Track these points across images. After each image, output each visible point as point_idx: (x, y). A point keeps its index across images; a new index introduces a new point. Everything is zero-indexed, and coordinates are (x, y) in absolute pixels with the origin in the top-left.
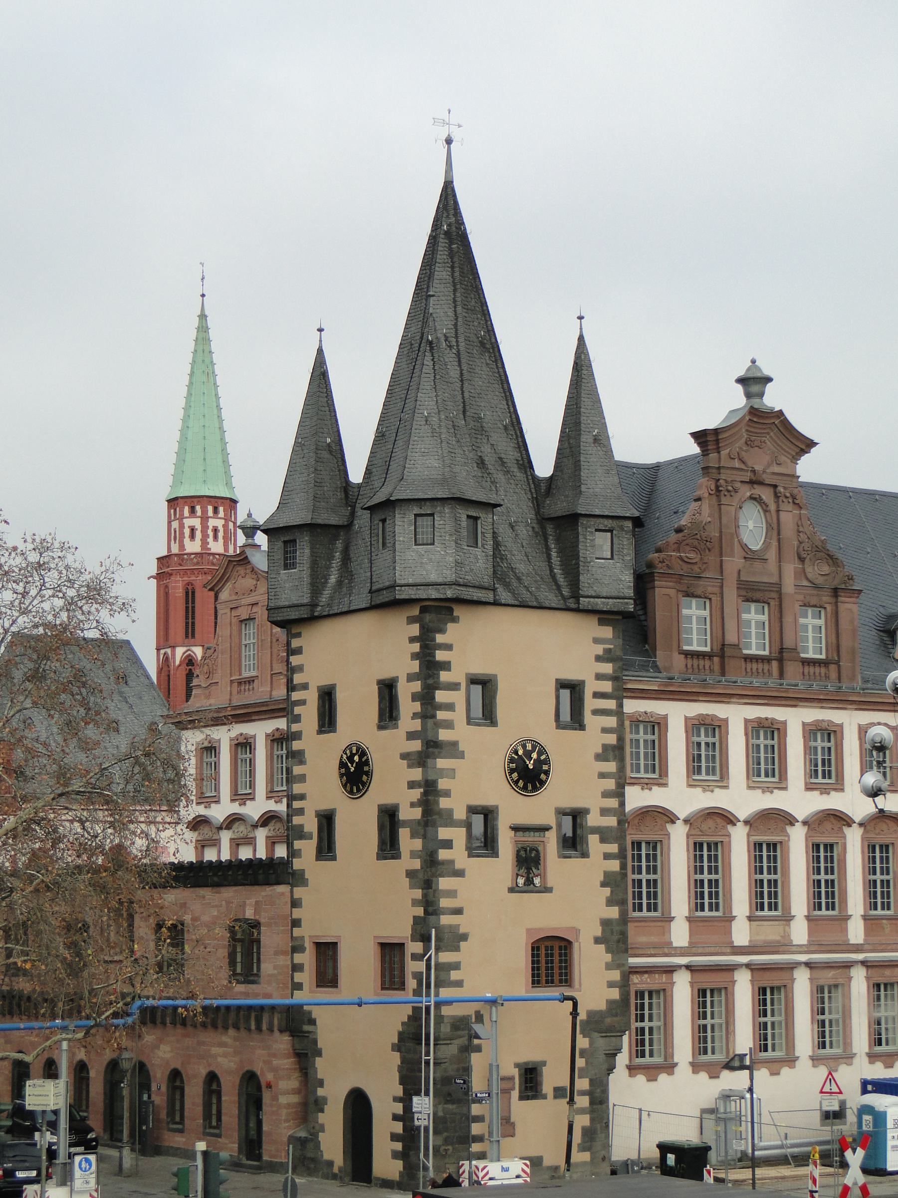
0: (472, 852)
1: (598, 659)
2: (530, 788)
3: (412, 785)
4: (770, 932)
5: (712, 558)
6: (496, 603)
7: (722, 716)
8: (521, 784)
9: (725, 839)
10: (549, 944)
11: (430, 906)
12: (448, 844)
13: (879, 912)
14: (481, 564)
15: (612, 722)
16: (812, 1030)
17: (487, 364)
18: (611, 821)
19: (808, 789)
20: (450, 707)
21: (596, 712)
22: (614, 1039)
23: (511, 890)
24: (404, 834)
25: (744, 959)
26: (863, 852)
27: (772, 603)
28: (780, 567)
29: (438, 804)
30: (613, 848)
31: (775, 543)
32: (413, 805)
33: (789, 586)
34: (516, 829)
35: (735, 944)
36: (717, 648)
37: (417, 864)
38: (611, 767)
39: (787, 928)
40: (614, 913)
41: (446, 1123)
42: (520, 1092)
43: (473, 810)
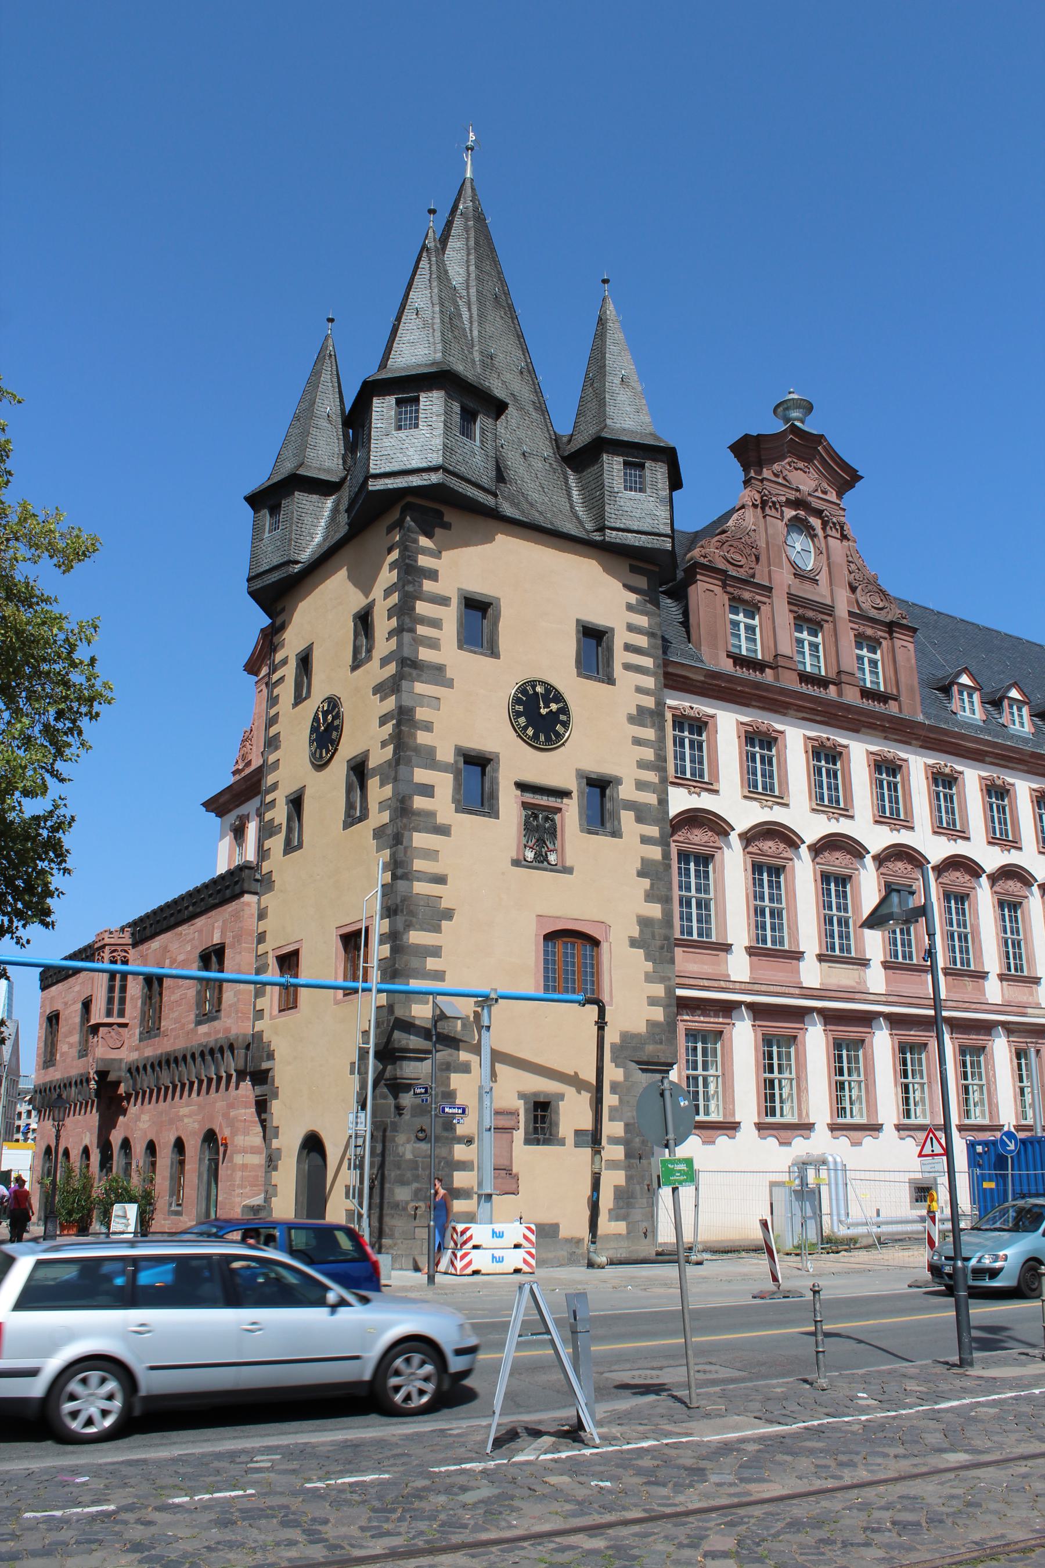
0: (463, 806)
2: (542, 738)
4: (842, 976)
8: (530, 732)
11: (399, 869)
12: (428, 791)
15: (649, 682)
16: (896, 1094)
20: (436, 623)
21: (628, 667)
23: (516, 863)
28: (832, 590)
29: (415, 738)
30: (654, 831)
31: (825, 569)
32: (384, 744)
39: (862, 973)
40: (655, 911)
41: (416, 1169)
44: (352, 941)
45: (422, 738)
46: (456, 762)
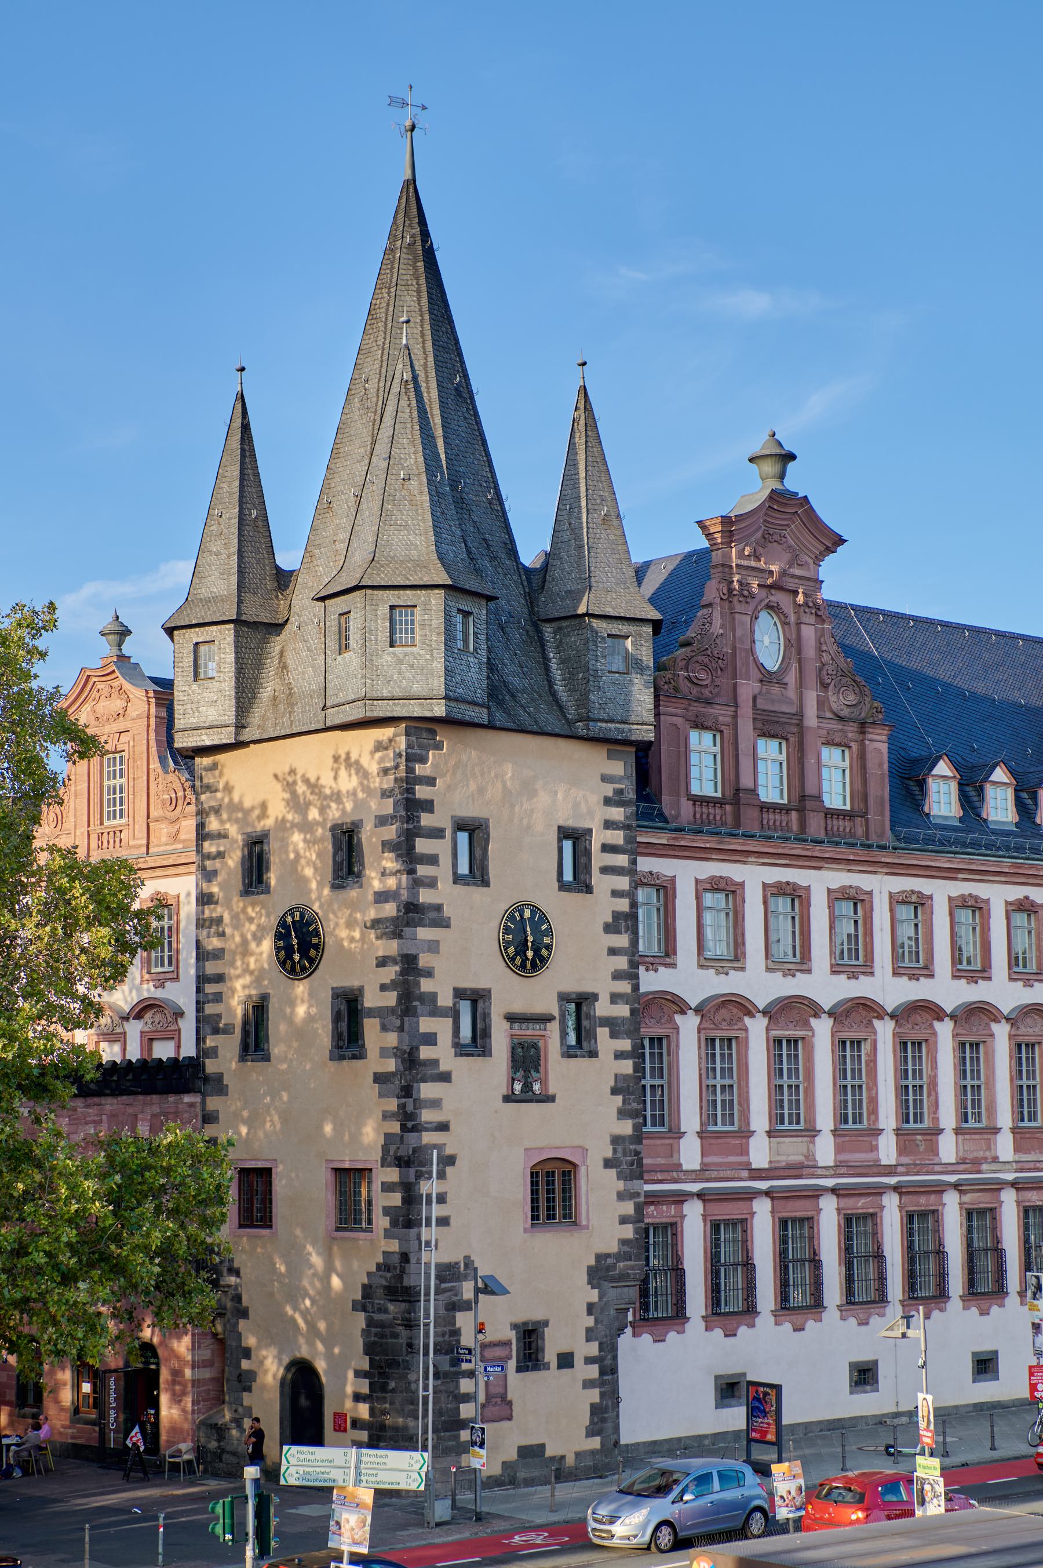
0: (461, 1050)
1: (608, 801)
3: (382, 962)
4: (792, 1150)
5: (724, 681)
6: (491, 726)
7: (738, 879)
9: (741, 1034)
10: (549, 1167)
12: (431, 1039)
13: (912, 1125)
14: (474, 674)
15: (623, 883)
17: (465, 418)
18: (623, 1011)
19: (833, 972)
21: (605, 870)
22: (626, 1290)
23: (507, 1099)
24: (371, 1028)
25: (763, 1185)
26: (894, 1051)
27: (792, 739)
30: (626, 1045)
32: (383, 988)
33: (811, 718)
34: (512, 1018)
35: (754, 1167)
36: (729, 793)
37: (391, 1065)
38: (622, 941)
40: (626, 1128)
42: (518, 1362)
43: (460, 994)
44: (348, 1179)
45: (426, 985)
46: (454, 1004)
